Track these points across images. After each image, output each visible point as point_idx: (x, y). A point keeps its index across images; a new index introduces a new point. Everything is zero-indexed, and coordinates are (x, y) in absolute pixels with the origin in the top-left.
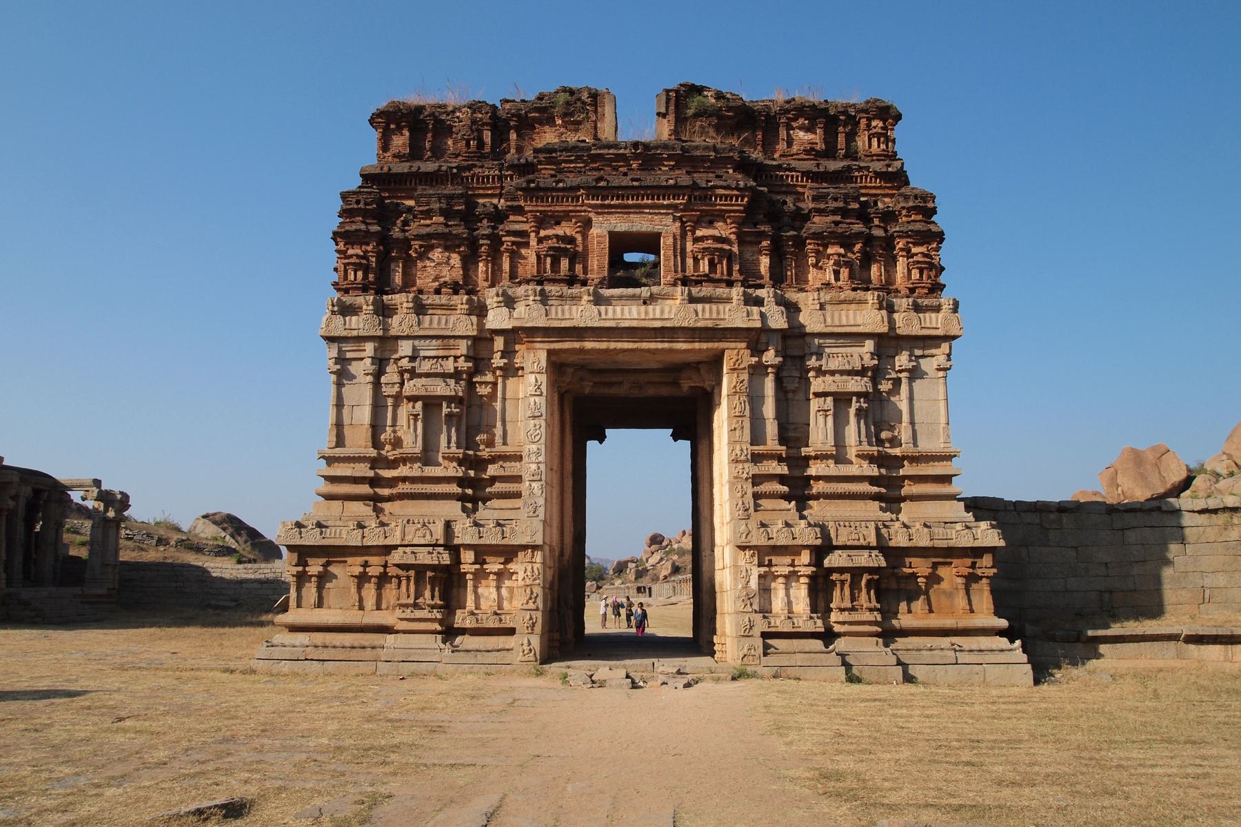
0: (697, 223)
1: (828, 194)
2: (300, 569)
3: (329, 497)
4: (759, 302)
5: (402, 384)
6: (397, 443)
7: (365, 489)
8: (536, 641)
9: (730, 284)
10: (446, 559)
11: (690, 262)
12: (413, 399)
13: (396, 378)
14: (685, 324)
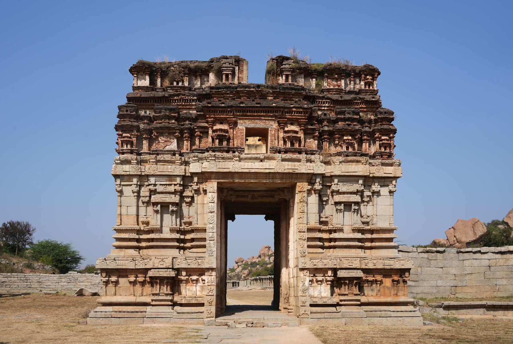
0: (286, 124)
1: (345, 111)
2: (107, 279)
3: (118, 247)
4: (311, 161)
5: (150, 197)
6: (147, 223)
7: (135, 244)
8: (213, 309)
9: (300, 153)
10: (173, 274)
11: (281, 142)
12: (155, 204)
13: (148, 194)
14: (280, 171)
